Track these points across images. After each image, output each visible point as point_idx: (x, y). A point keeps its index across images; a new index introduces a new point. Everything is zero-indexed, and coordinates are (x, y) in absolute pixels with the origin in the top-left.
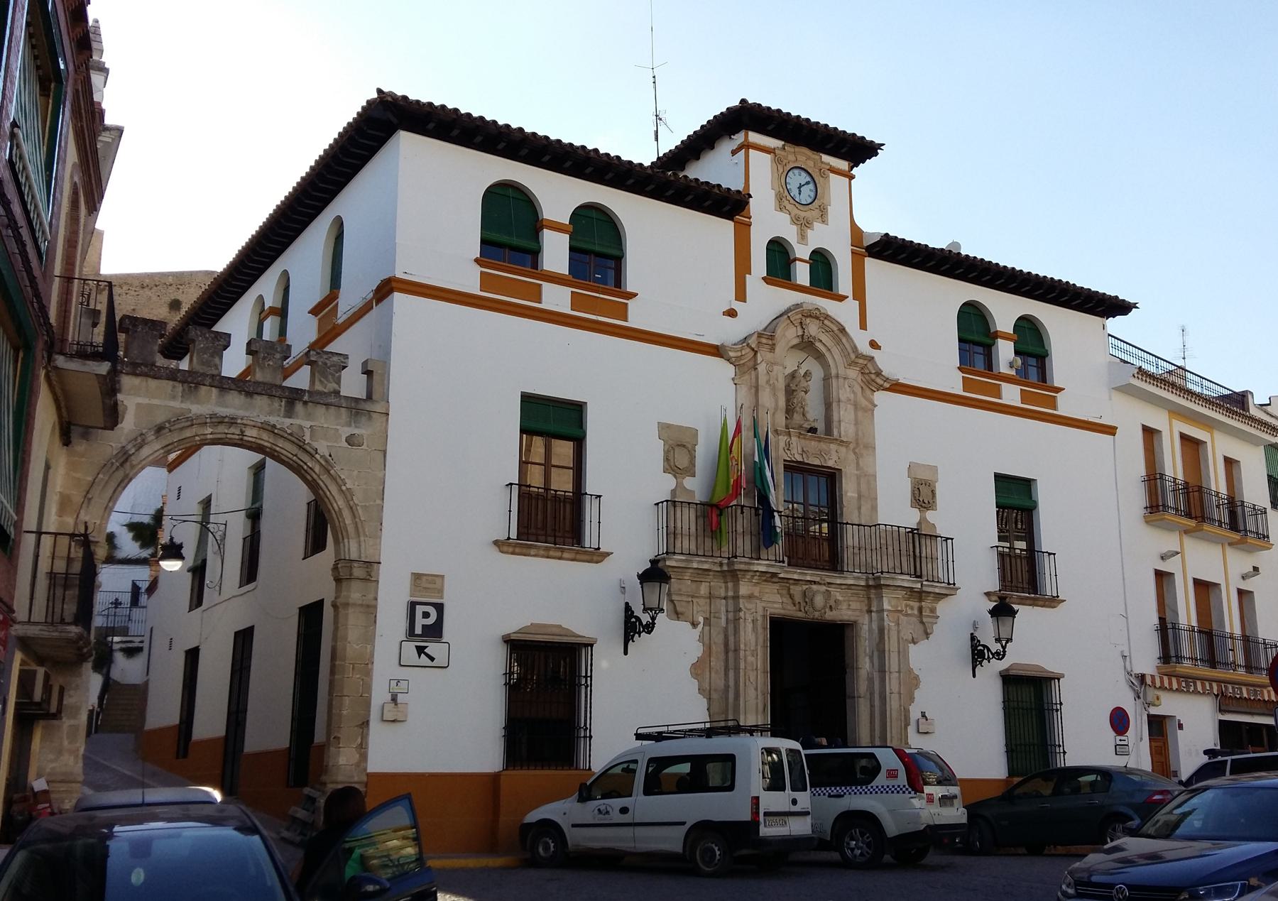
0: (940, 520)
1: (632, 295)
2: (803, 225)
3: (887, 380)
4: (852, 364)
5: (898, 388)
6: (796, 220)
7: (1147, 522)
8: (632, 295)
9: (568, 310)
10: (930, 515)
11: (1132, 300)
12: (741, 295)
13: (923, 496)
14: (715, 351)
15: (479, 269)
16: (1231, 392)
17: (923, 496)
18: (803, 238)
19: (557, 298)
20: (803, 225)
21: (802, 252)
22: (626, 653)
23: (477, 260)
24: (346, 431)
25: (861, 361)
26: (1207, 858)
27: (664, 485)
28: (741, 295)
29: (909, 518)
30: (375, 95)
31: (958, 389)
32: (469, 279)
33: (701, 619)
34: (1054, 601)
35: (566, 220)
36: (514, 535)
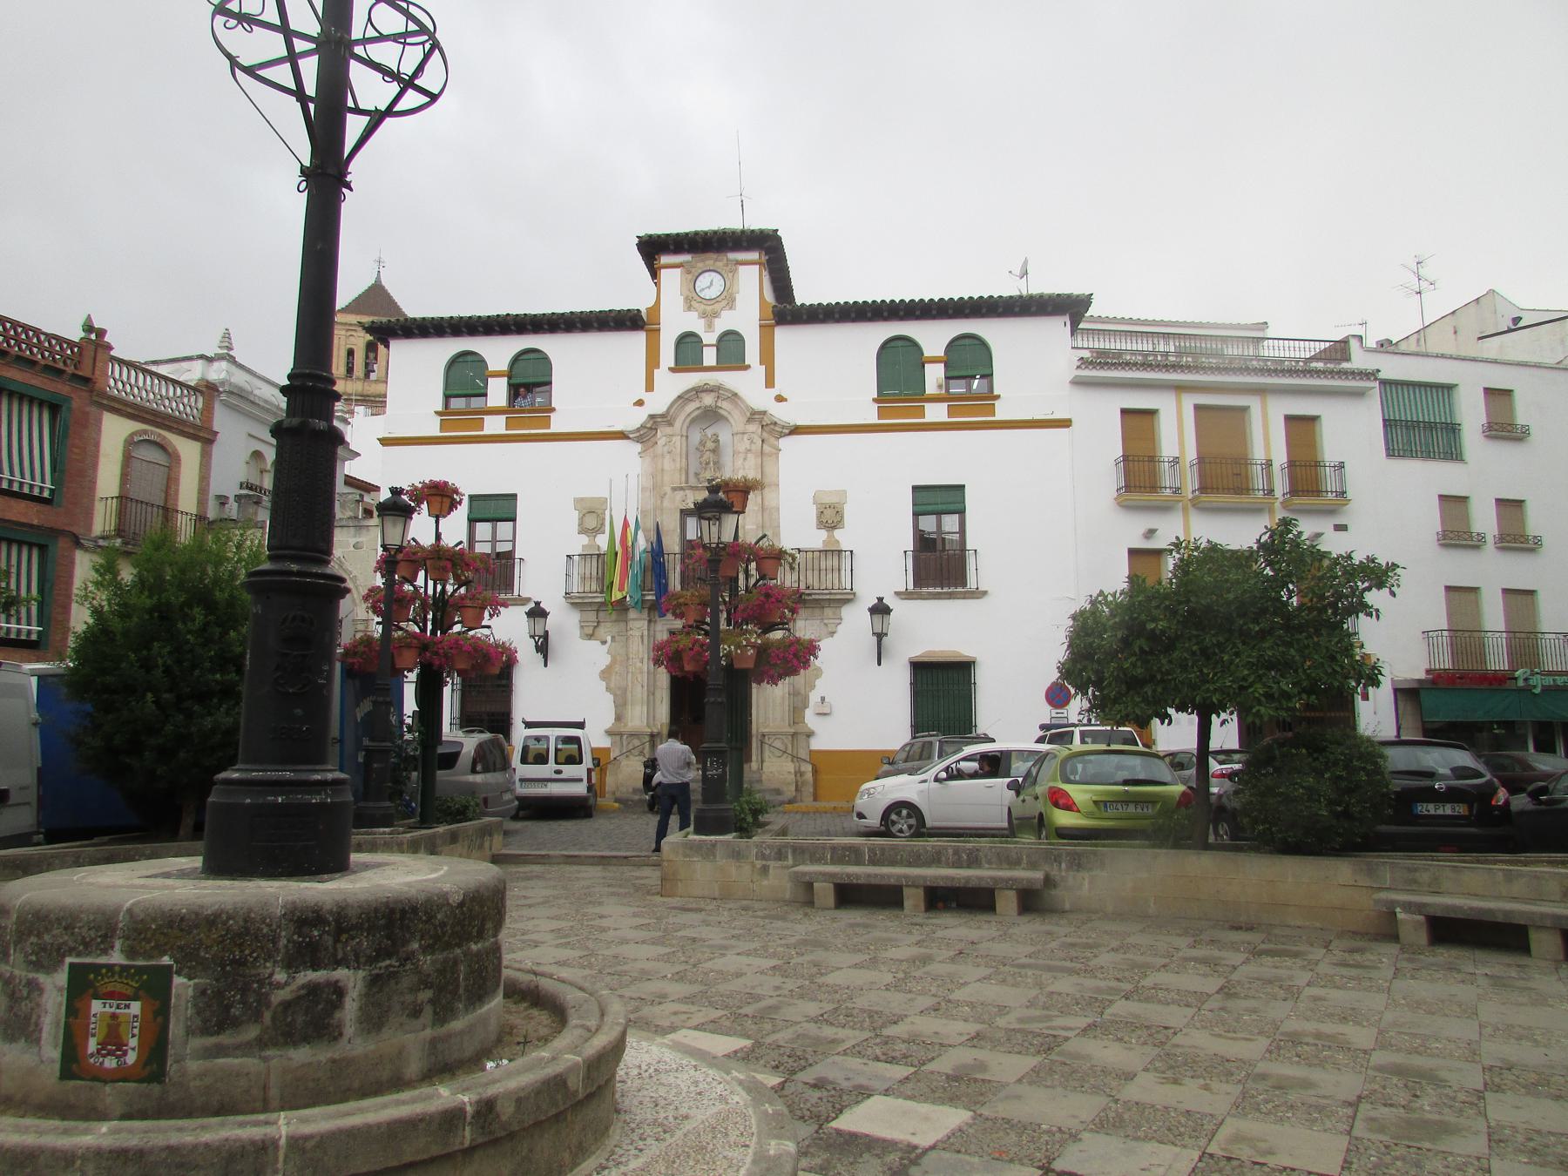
0: (844, 538)
1: (998, 397)
2: (710, 317)
3: (783, 427)
4: (750, 420)
5: (796, 430)
6: (704, 315)
7: (1119, 504)
8: (998, 397)
9: (946, 419)
10: (837, 533)
11: (85, 317)
12: (650, 387)
13: (830, 518)
14: (621, 435)
15: (876, 405)
16: (1328, 344)
17: (830, 518)
18: (710, 327)
19: (936, 412)
20: (710, 317)
21: (710, 338)
22: (879, 664)
23: (874, 400)
24: (353, 541)
25: (757, 416)
26: (149, 873)
27: (578, 544)
28: (650, 387)
29: (816, 539)
30: (76, 335)
31: (872, 418)
32: (871, 416)
33: (609, 639)
34: (978, 594)
35: (941, 353)
36: (911, 587)
